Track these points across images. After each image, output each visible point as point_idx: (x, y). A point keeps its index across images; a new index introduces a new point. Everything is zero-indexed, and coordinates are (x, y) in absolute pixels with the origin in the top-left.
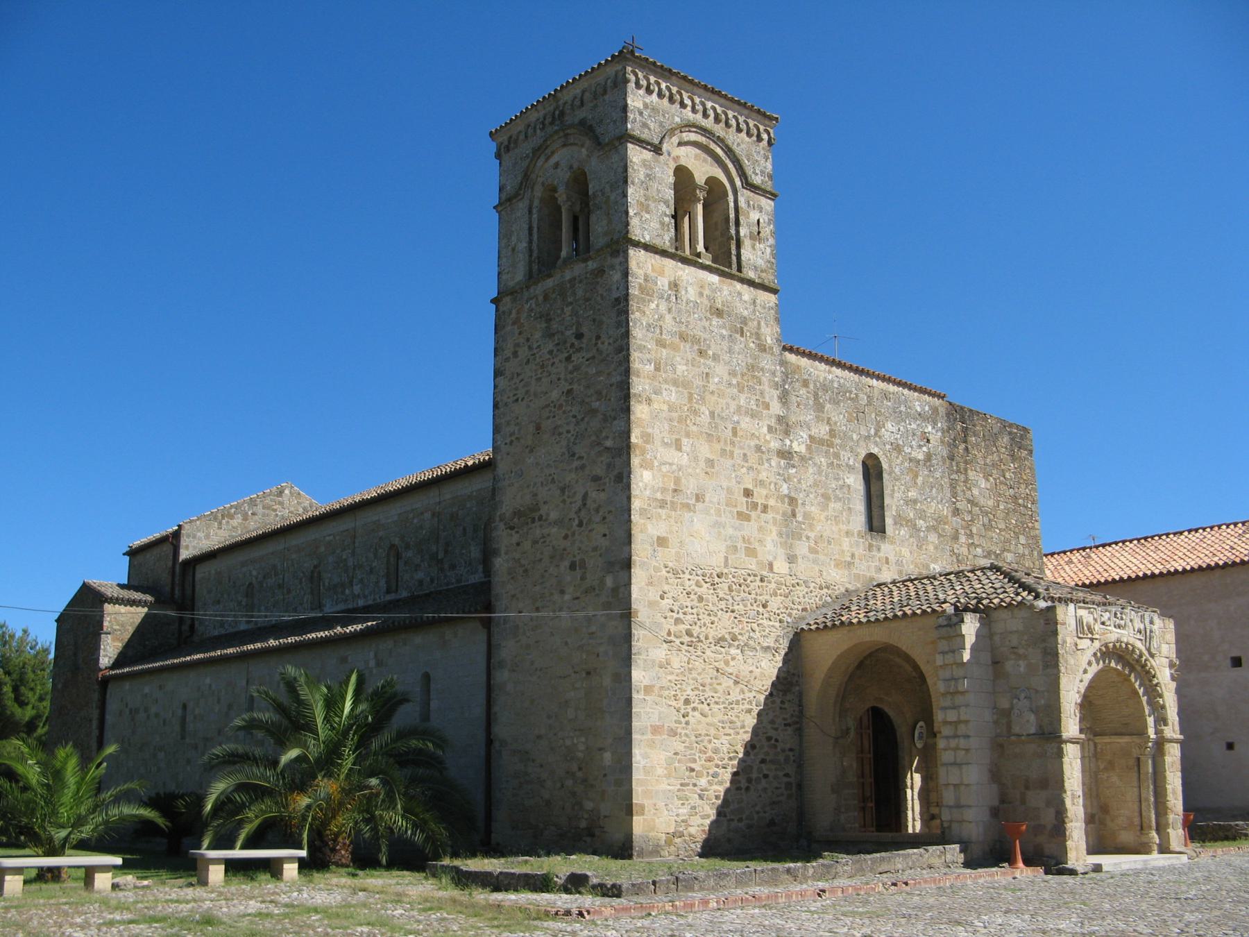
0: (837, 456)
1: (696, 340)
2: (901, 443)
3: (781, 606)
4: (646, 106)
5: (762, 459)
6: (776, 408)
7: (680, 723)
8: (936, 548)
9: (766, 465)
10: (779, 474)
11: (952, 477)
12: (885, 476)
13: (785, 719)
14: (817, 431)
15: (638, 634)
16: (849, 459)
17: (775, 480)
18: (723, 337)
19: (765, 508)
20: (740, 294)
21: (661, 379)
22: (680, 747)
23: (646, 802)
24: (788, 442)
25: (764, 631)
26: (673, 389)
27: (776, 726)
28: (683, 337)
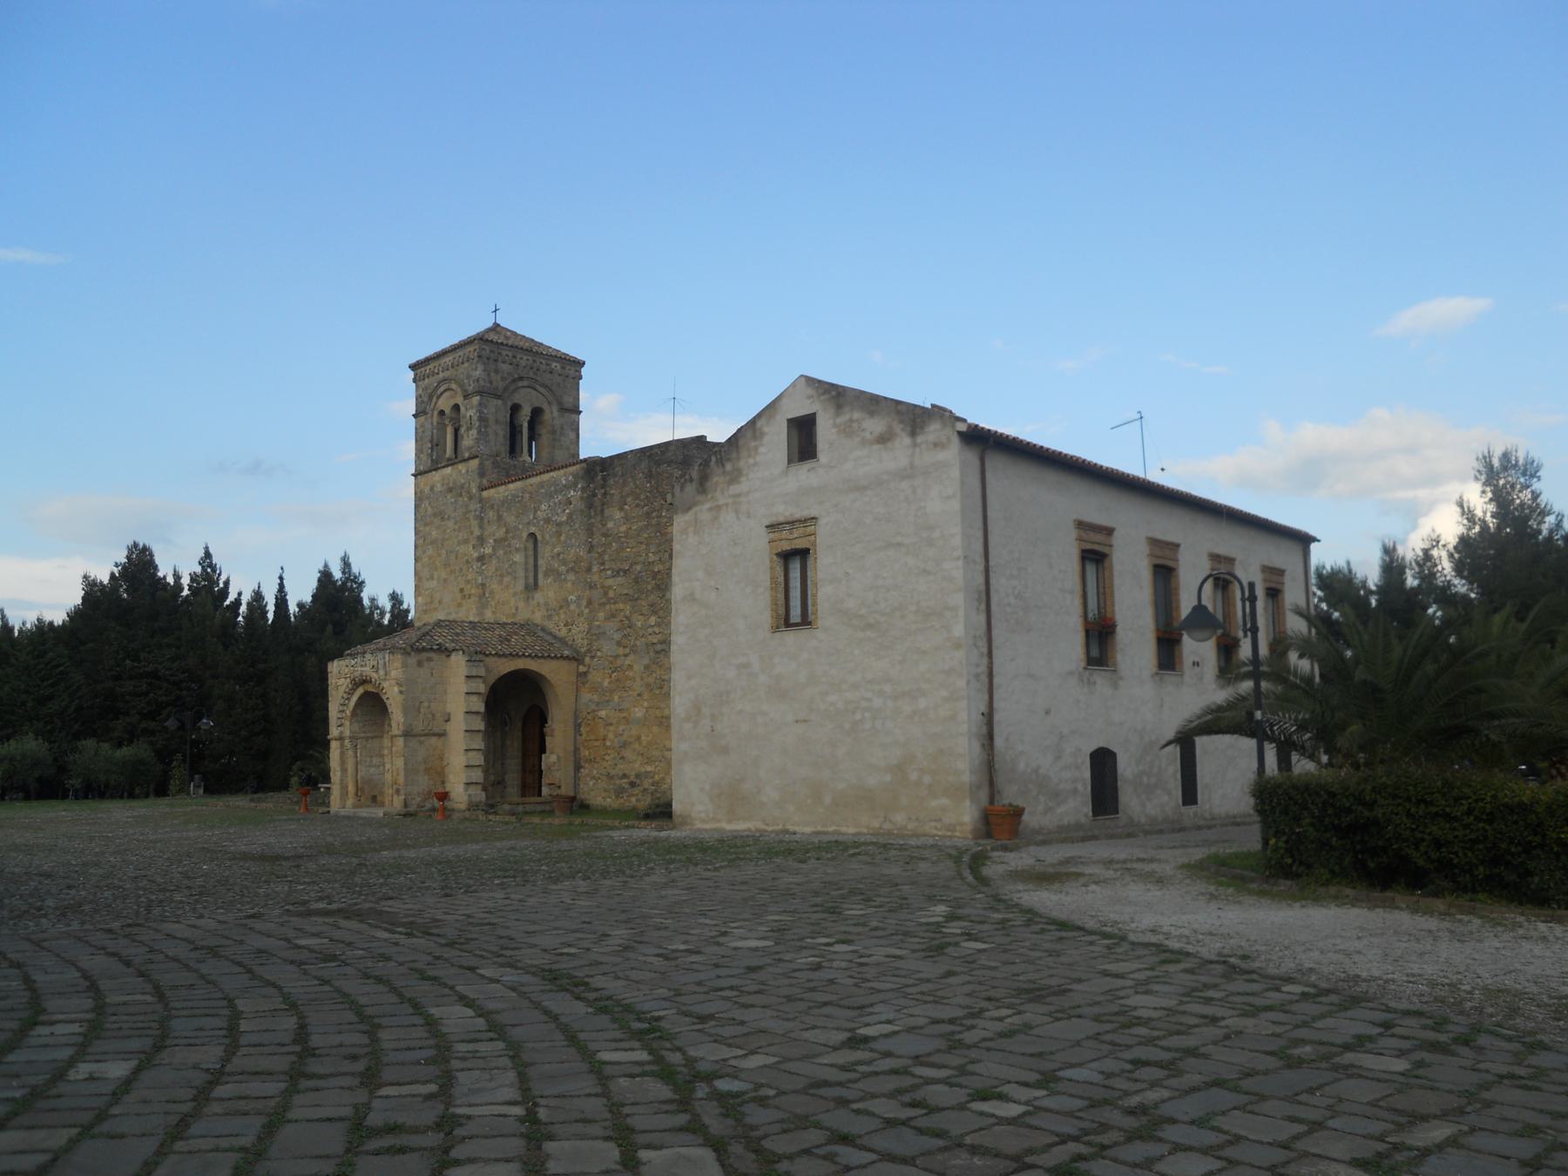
0: (509, 545)
6: (477, 532)
20: (460, 471)
28: (435, 515)
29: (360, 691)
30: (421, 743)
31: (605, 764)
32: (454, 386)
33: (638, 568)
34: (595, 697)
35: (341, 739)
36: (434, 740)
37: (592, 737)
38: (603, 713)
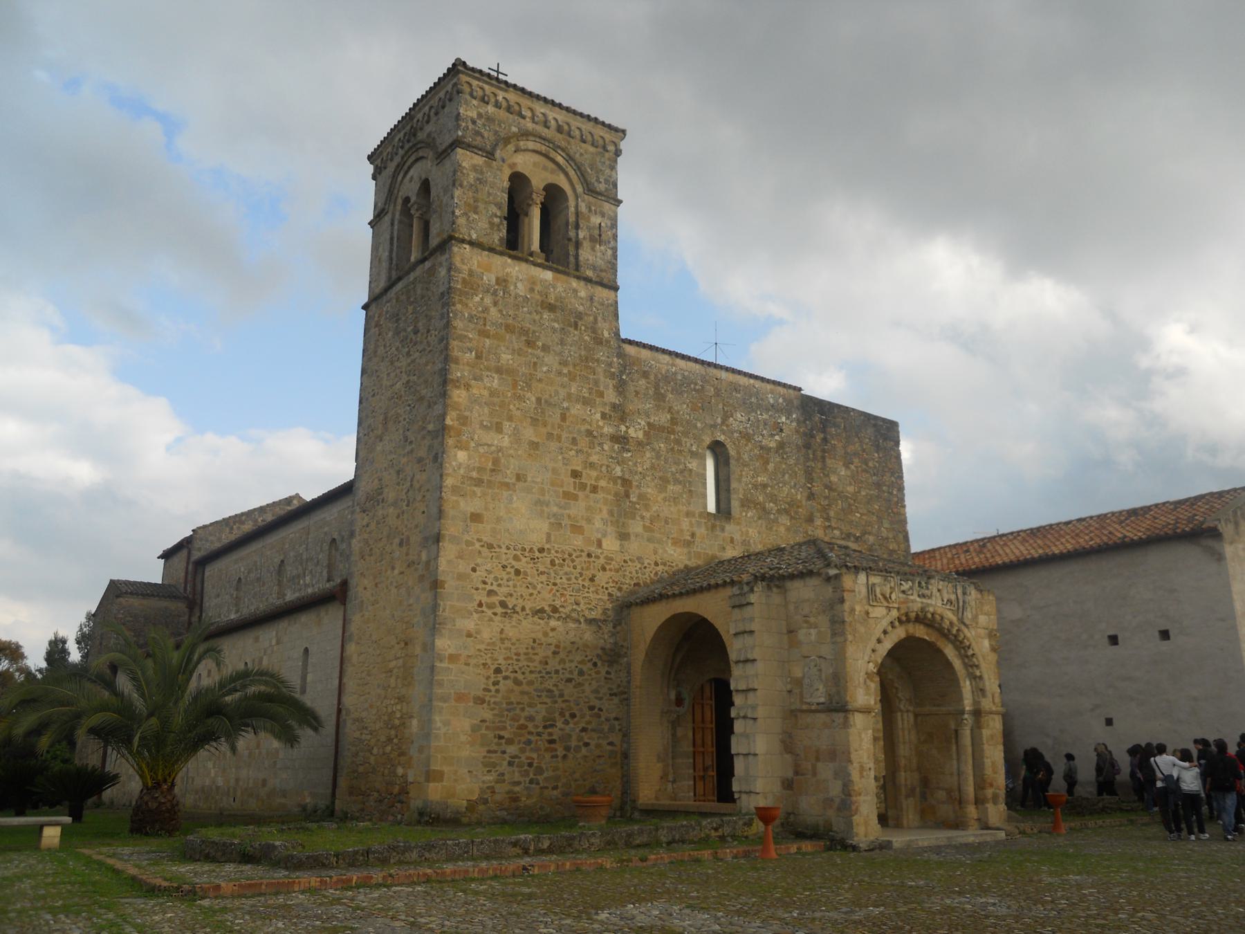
0: (678, 442)
1: (523, 332)
2: (751, 432)
3: (611, 580)
4: (480, 115)
5: (593, 443)
6: (611, 396)
7: (489, 691)
8: (788, 529)
9: (598, 449)
10: (612, 458)
11: (808, 464)
12: (732, 462)
13: (610, 689)
14: (656, 419)
15: (444, 604)
16: (692, 445)
17: (607, 463)
18: (554, 330)
19: (595, 489)
20: (575, 291)
21: (482, 366)
22: (488, 715)
23: (446, 769)
24: (623, 428)
25: (590, 604)
26: (496, 376)
27: (601, 695)
28: (509, 328)
32: (559, 159)
33: (871, 539)
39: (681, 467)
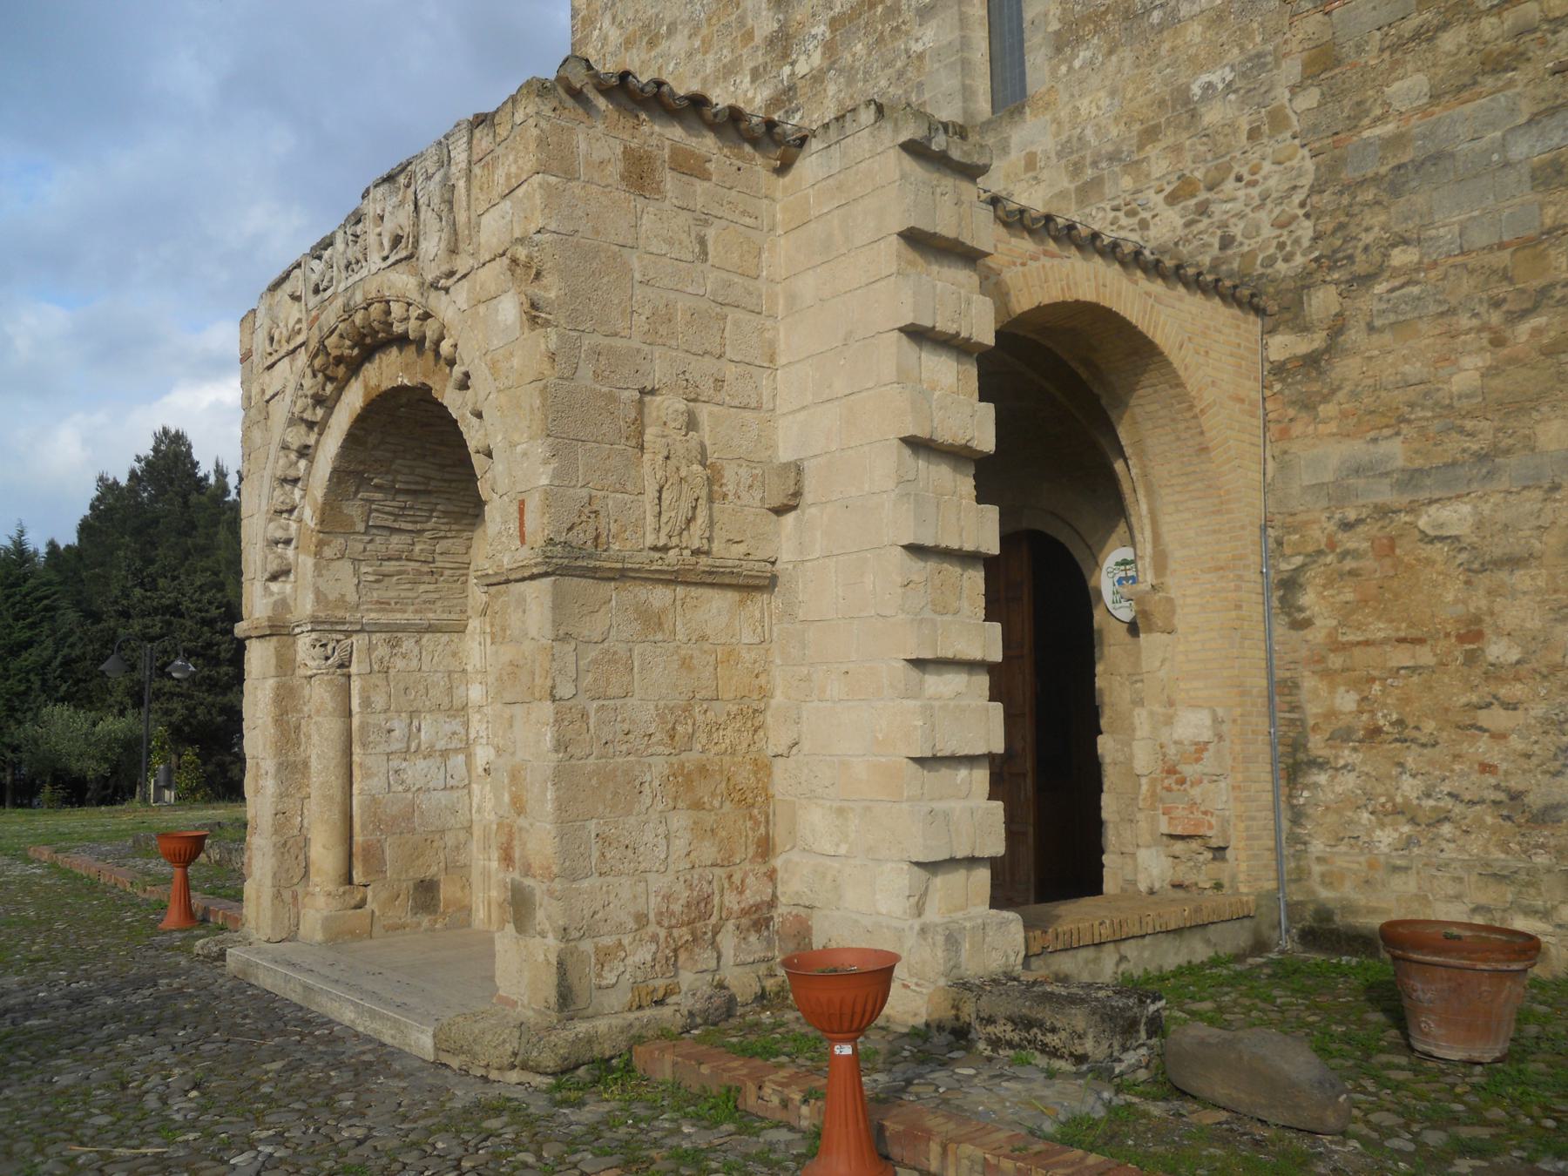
29: (353, 399)
30: (652, 621)
31: (1483, 747)
34: (1395, 451)
35: (278, 630)
36: (716, 606)
37: (1379, 629)
38: (1456, 516)
39: (899, 64)
